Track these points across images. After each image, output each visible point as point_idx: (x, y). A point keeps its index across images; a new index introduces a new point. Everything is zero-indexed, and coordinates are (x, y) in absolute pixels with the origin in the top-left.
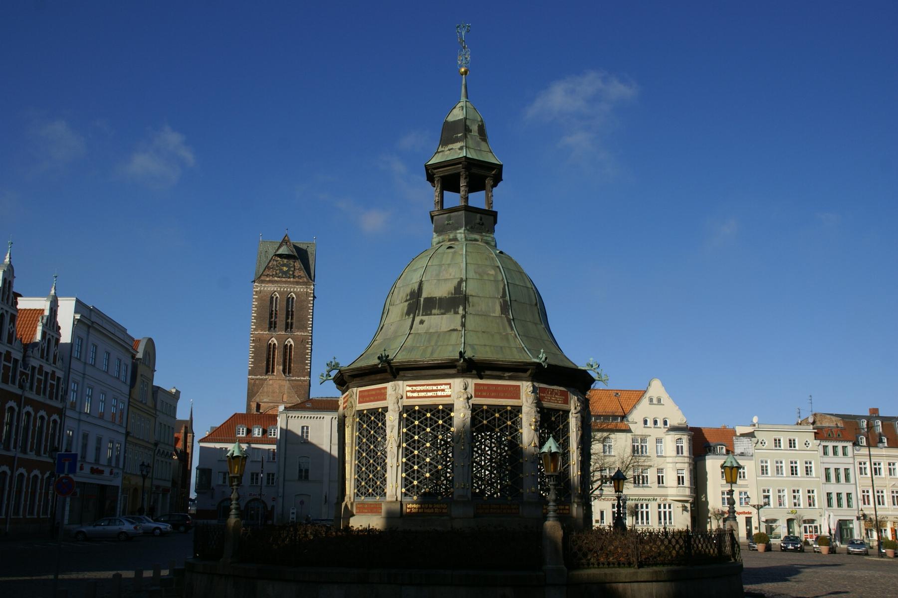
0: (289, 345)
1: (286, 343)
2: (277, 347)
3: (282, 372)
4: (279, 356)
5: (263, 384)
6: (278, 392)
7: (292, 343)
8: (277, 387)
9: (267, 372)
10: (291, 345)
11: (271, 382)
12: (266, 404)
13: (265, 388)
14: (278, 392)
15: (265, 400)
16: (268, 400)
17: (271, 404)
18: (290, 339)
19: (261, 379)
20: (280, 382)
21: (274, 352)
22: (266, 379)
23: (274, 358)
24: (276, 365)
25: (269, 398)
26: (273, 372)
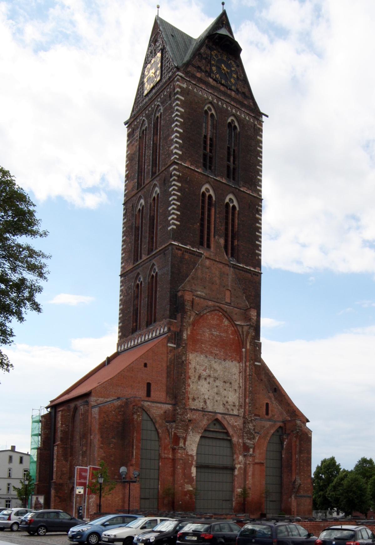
0: (231, 205)
1: (227, 200)
2: (214, 202)
3: (224, 250)
4: (218, 220)
5: (195, 263)
6: (218, 282)
7: (235, 203)
8: (217, 273)
9: (201, 244)
10: (234, 207)
11: (208, 262)
12: (202, 300)
13: (199, 272)
14: (218, 282)
15: (199, 293)
16: (204, 295)
17: (210, 303)
18: (231, 196)
19: (193, 253)
20: (221, 266)
21: (209, 210)
22: (200, 255)
23: (209, 222)
24: (212, 234)
25: (205, 291)
26: (209, 246)
